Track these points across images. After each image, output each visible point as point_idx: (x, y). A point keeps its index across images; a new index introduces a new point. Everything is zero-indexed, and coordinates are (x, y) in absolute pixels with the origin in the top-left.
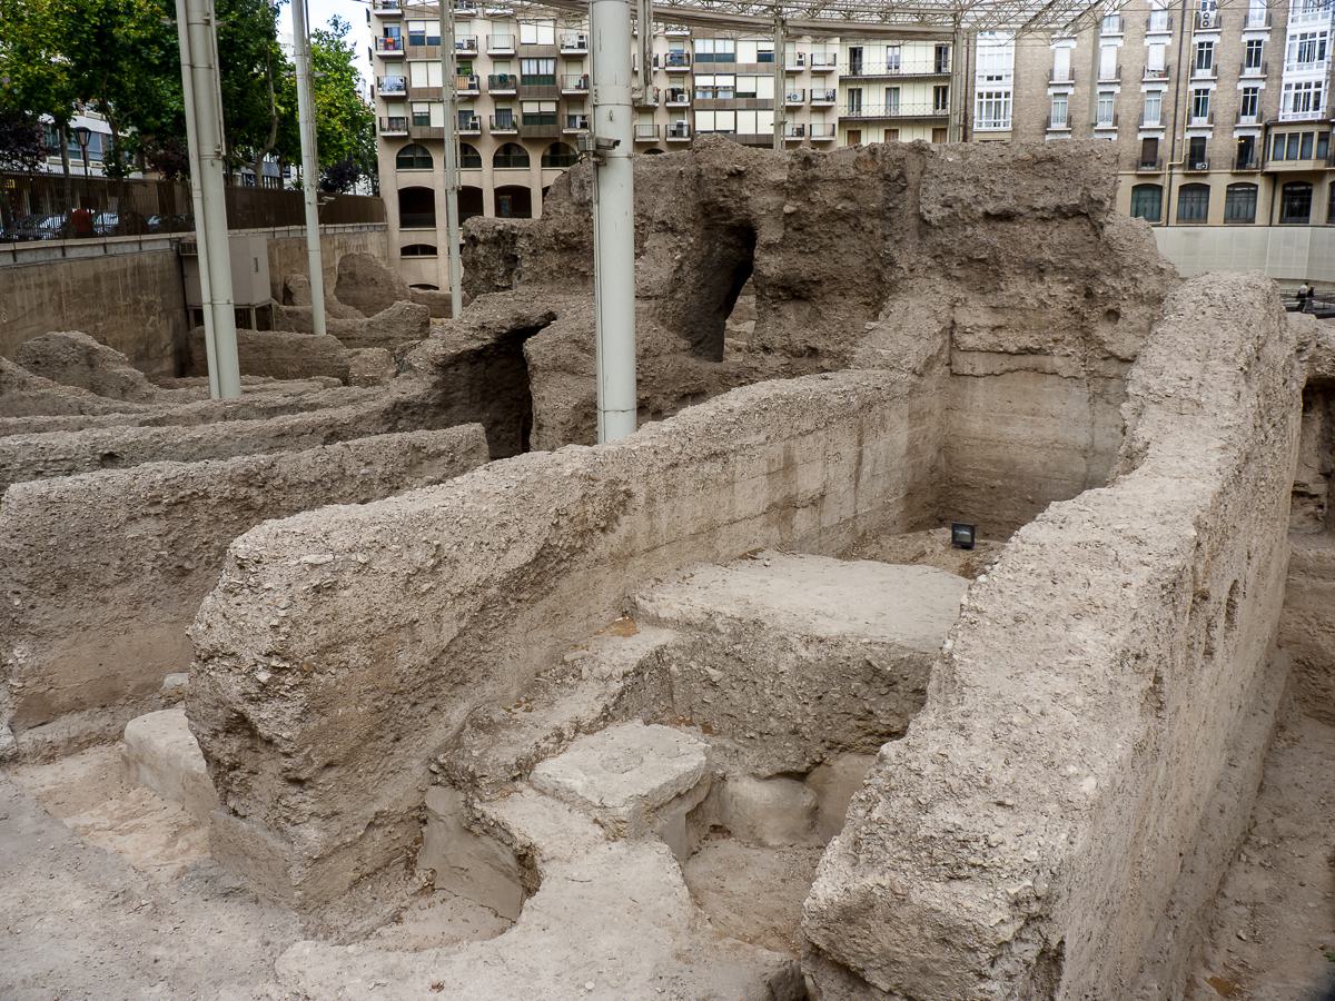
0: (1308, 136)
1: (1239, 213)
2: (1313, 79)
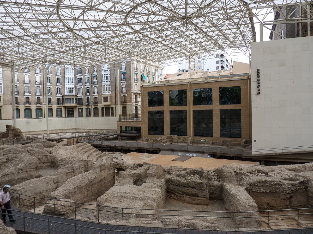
0: (73, 98)
1: (59, 115)
2: (72, 87)
